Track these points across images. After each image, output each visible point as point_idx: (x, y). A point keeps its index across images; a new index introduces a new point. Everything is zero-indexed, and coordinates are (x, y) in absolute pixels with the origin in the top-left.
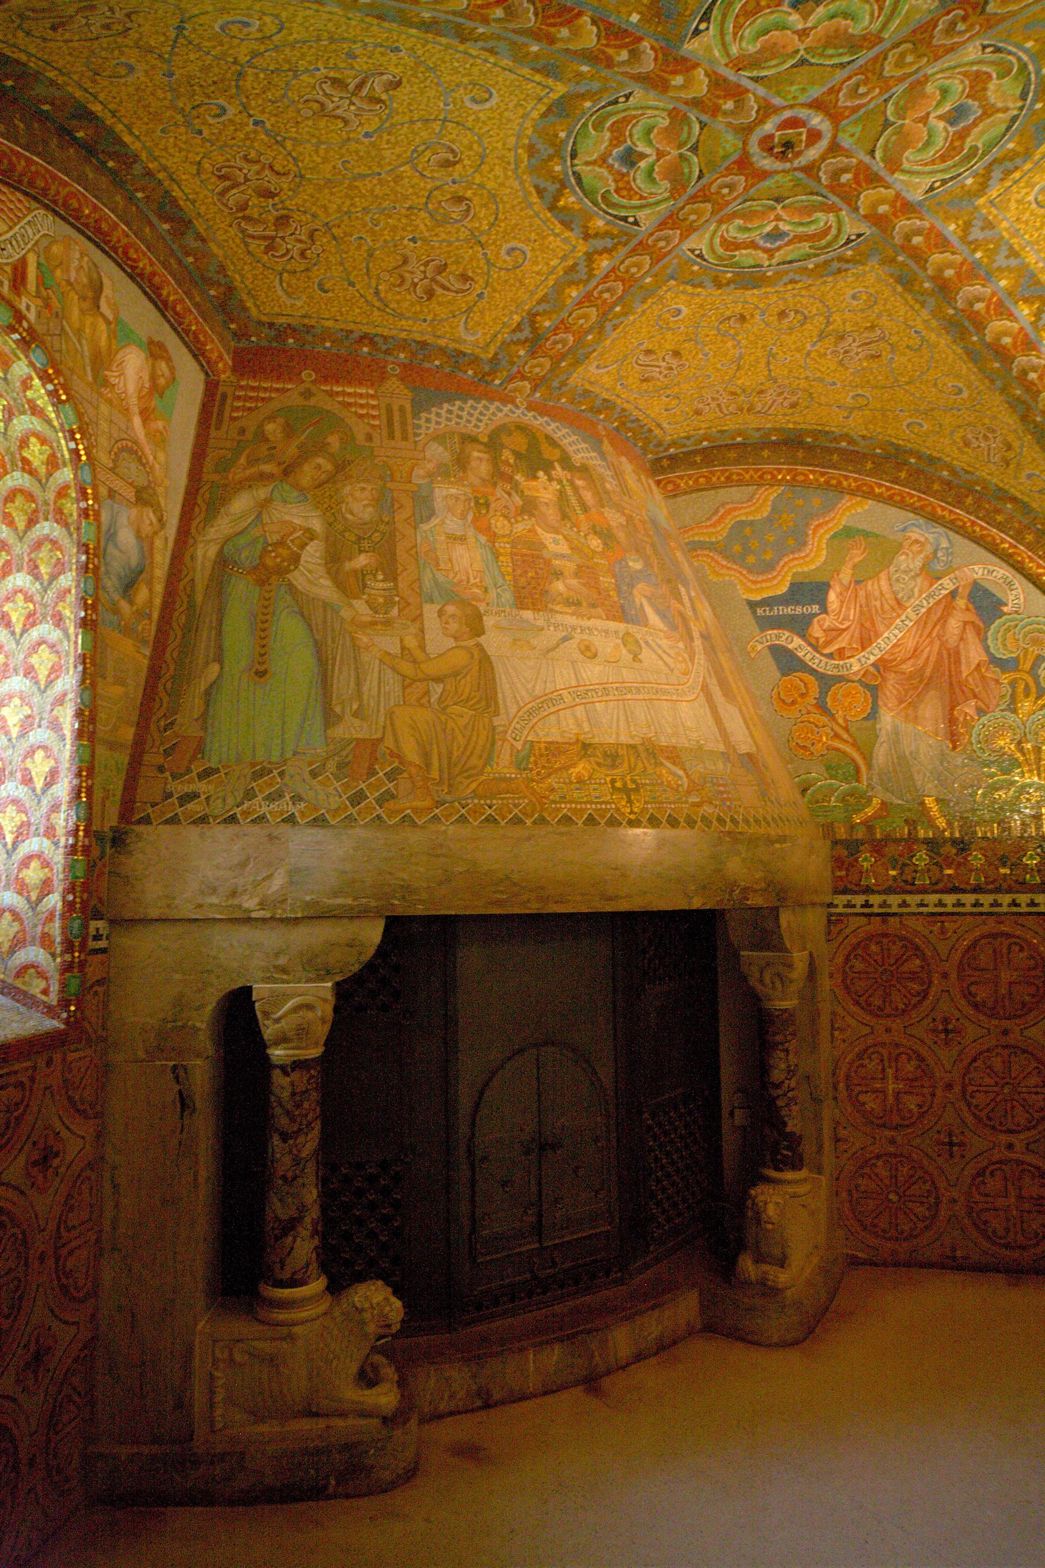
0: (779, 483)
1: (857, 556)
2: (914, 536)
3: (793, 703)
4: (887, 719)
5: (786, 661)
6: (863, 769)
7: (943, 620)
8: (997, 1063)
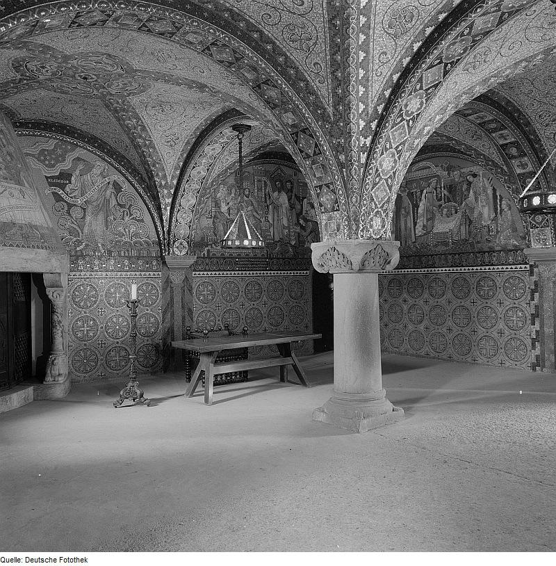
0: (57, 139)
1: (81, 167)
2: (98, 164)
3: (60, 211)
4: (88, 218)
5: (58, 198)
6: (81, 234)
7: (105, 190)
8: (114, 320)
